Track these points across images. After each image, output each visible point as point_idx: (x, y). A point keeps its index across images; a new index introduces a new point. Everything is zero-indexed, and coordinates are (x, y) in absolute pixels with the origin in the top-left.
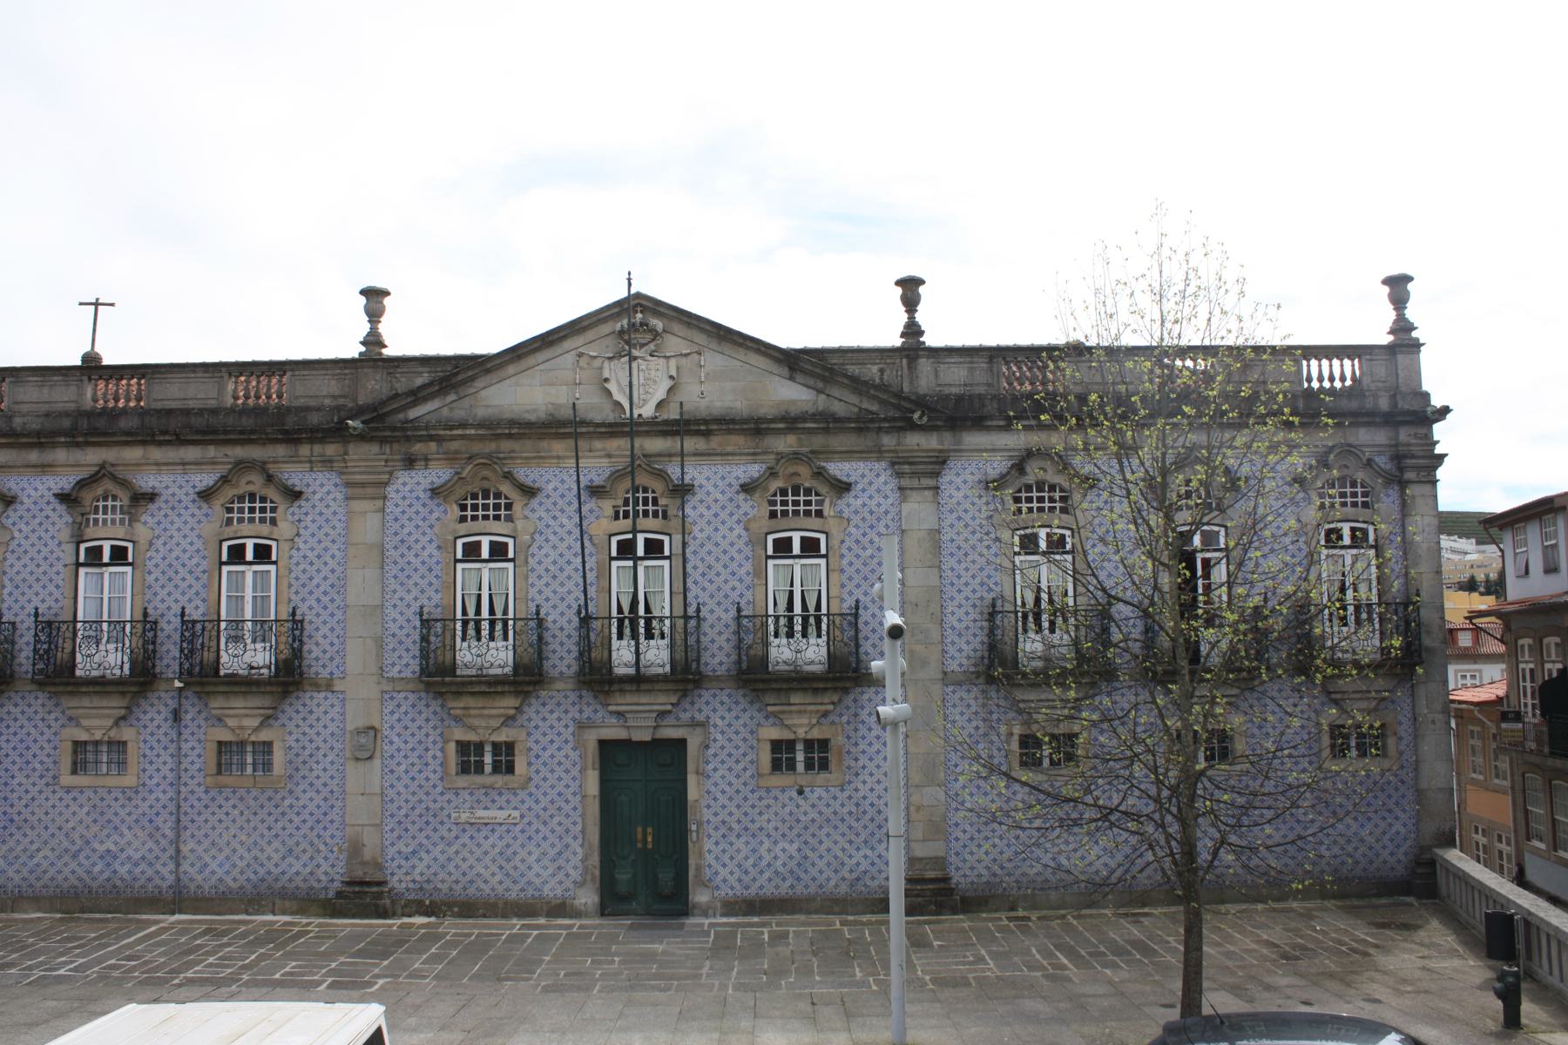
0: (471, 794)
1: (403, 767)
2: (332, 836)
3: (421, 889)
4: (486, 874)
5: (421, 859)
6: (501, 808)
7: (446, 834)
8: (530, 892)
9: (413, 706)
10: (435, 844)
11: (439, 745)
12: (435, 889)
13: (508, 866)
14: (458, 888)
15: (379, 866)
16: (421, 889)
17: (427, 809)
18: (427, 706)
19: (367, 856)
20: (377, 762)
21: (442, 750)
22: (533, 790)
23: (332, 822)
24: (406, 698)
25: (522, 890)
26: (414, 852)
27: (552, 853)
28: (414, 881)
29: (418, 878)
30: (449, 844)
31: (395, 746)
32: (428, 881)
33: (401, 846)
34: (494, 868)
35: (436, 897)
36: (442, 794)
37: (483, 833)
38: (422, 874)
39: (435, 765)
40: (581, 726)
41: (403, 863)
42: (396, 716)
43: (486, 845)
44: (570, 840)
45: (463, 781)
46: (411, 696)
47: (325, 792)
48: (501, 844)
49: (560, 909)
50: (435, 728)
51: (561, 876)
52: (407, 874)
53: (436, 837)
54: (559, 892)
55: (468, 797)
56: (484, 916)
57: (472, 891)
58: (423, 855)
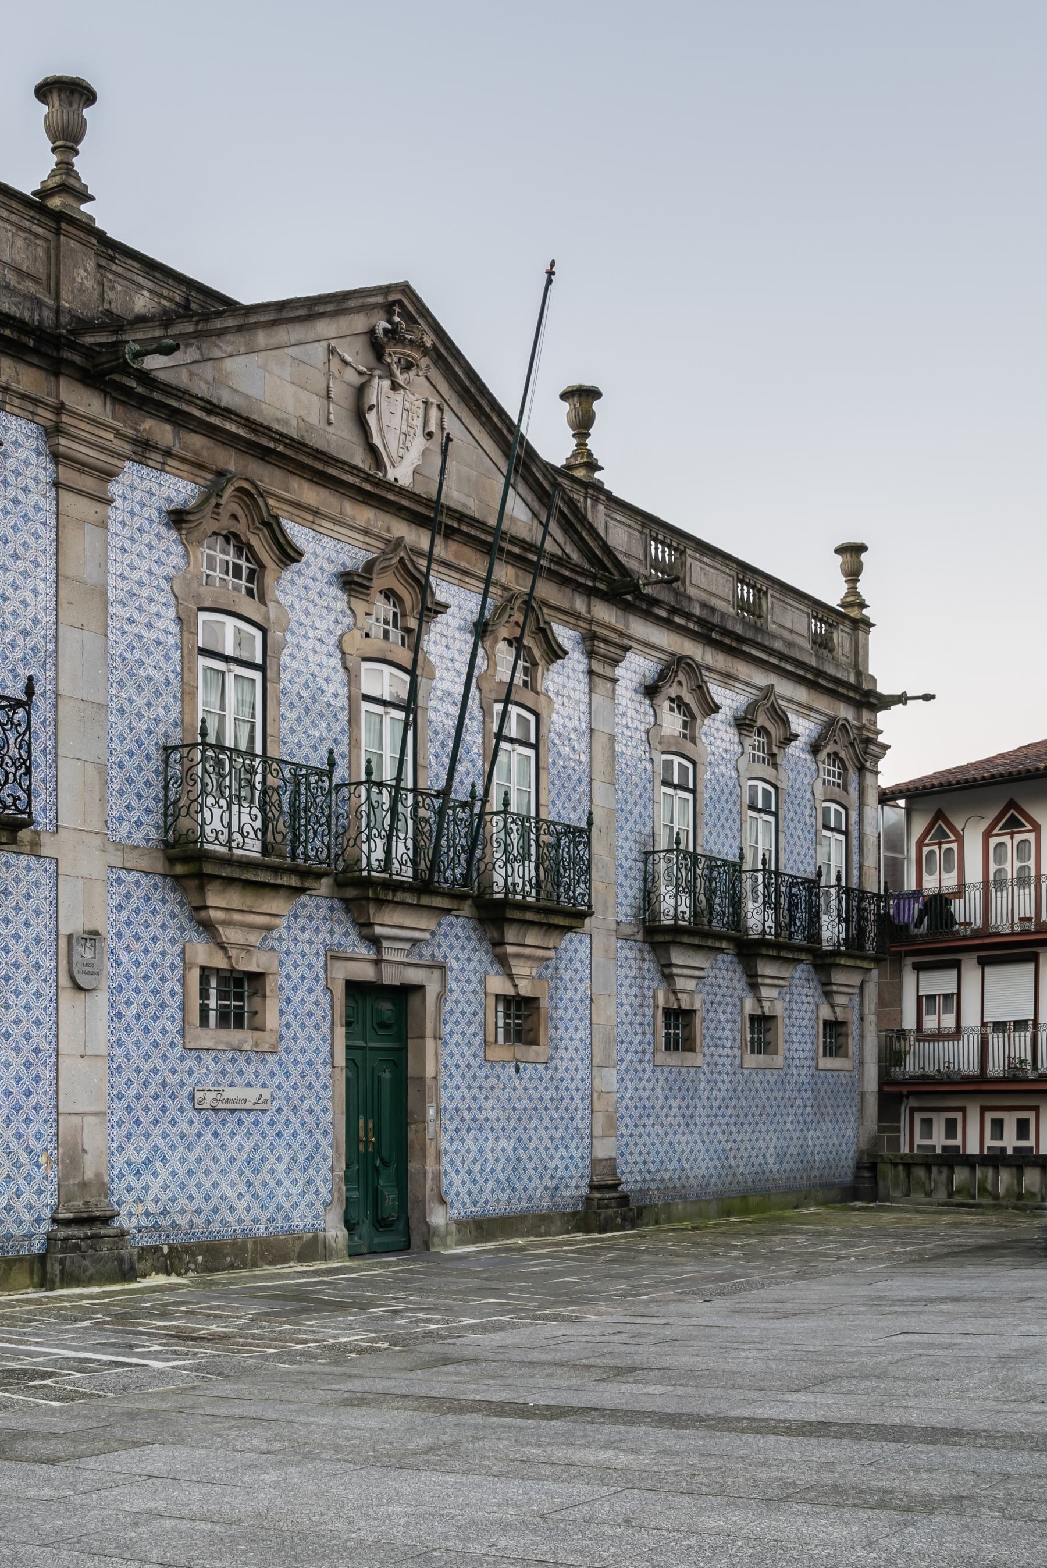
0: (216, 1060)
1: (134, 1009)
2: (39, 1136)
3: (156, 1227)
4: (232, 1195)
5: (155, 1174)
6: (249, 1085)
7: (184, 1126)
8: (280, 1223)
9: (147, 899)
10: (172, 1147)
11: (179, 972)
12: (175, 1226)
13: (256, 1182)
14: (199, 1221)
15: (104, 1190)
16: (156, 1227)
17: (164, 1084)
18: (164, 901)
19: (89, 1175)
20: (101, 999)
21: (183, 981)
22: (283, 1055)
23: (37, 1108)
24: (137, 884)
25: (272, 1220)
26: (148, 1162)
27: (303, 1157)
28: (147, 1214)
29: (152, 1209)
30: (190, 1147)
31: (122, 971)
32: (165, 1213)
33: (130, 1152)
34: (241, 1186)
35: (178, 1239)
36: (182, 1058)
37: (230, 1126)
38: (157, 1201)
39: (173, 1004)
40: (334, 956)
41: (132, 1180)
42: (124, 915)
43: (233, 1144)
44: (320, 1137)
45: (212, 1036)
46: (145, 881)
47: (27, 1053)
48: (249, 1145)
49: (312, 1248)
50: (173, 941)
51: (310, 1196)
52: (139, 1201)
53: (174, 1132)
54: (309, 1221)
55: (211, 1065)
56: (232, 1267)
57: (216, 1226)
58: (158, 1165)
